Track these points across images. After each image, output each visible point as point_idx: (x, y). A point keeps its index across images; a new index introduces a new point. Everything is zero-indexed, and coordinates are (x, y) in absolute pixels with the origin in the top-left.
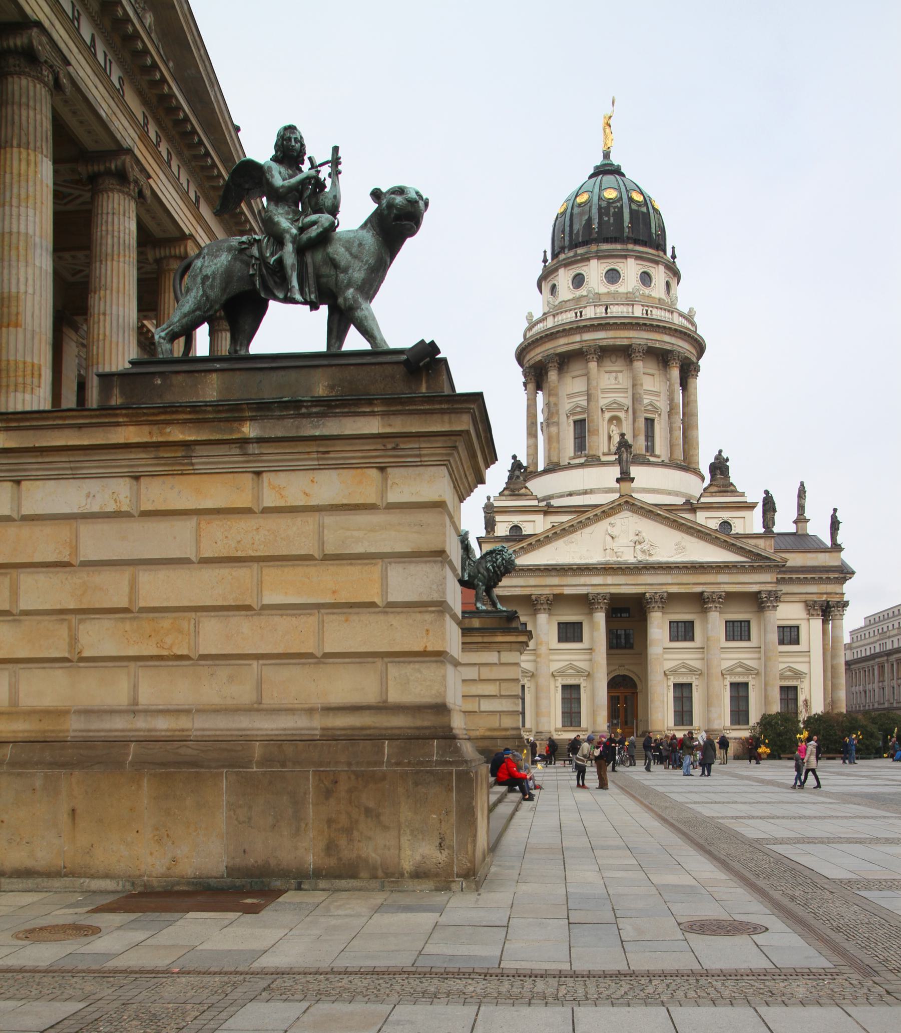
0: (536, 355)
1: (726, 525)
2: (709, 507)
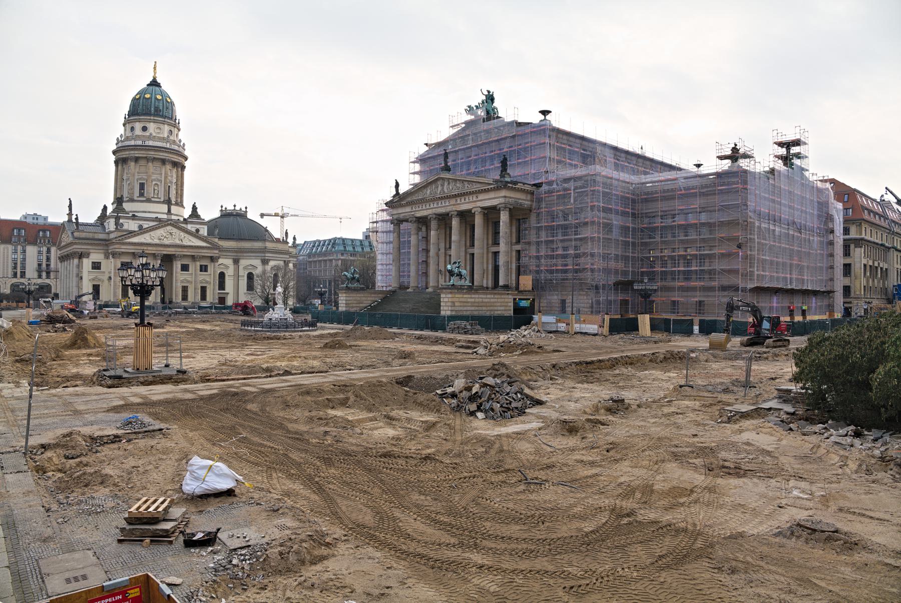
0: (124, 154)
1: (198, 231)
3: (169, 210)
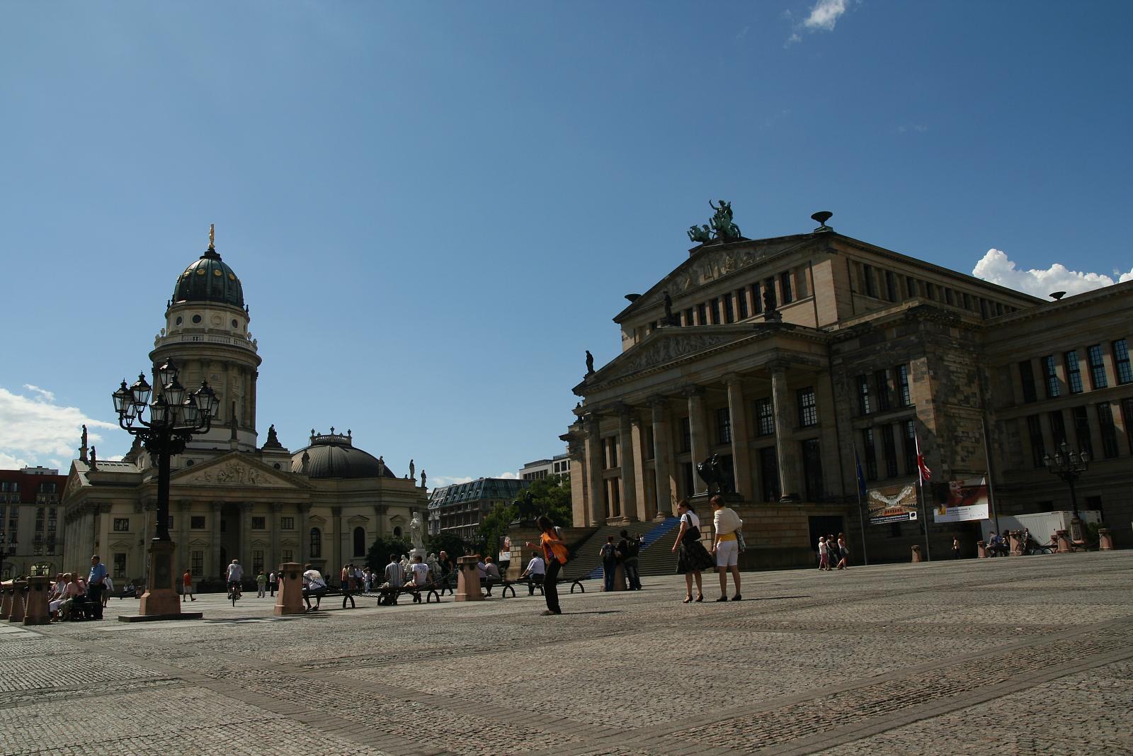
1: (277, 466)
2: (268, 455)
3: (234, 437)
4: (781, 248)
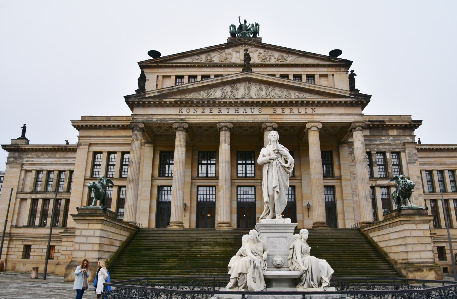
4: (310, 61)
